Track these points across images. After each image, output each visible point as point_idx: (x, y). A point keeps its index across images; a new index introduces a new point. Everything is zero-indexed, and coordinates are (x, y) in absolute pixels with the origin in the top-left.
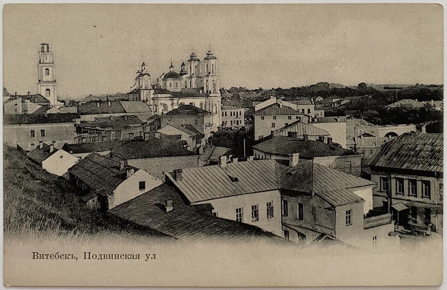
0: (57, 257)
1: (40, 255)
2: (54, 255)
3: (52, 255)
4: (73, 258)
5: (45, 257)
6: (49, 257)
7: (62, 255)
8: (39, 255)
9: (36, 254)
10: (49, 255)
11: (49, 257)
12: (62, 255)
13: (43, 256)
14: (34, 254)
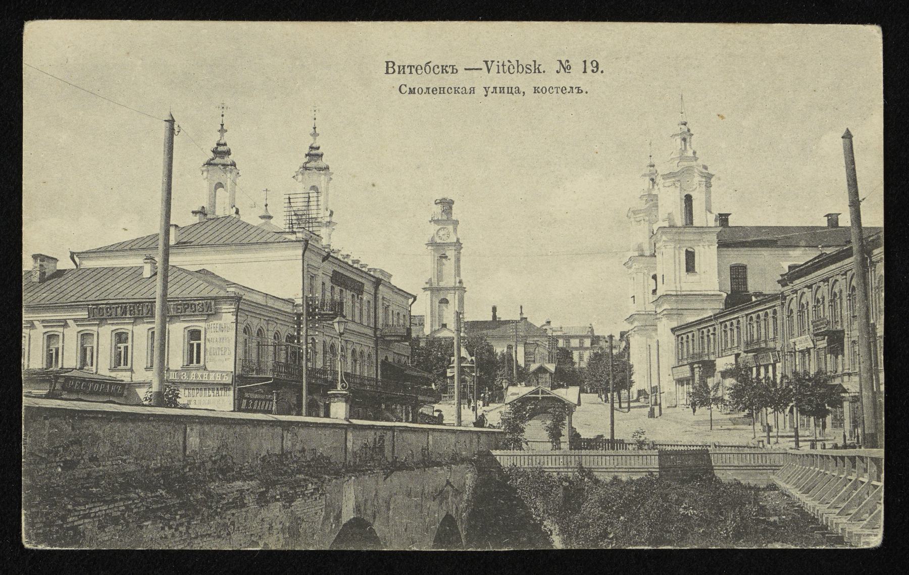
0: (427, 68)
1: (399, 67)
2: (423, 69)
3: (419, 68)
4: (455, 71)
5: (407, 70)
6: (414, 70)
7: (436, 67)
8: (396, 68)
9: (391, 65)
10: (414, 66)
11: (414, 70)
12: (436, 67)
13: (404, 68)
14: (387, 65)
